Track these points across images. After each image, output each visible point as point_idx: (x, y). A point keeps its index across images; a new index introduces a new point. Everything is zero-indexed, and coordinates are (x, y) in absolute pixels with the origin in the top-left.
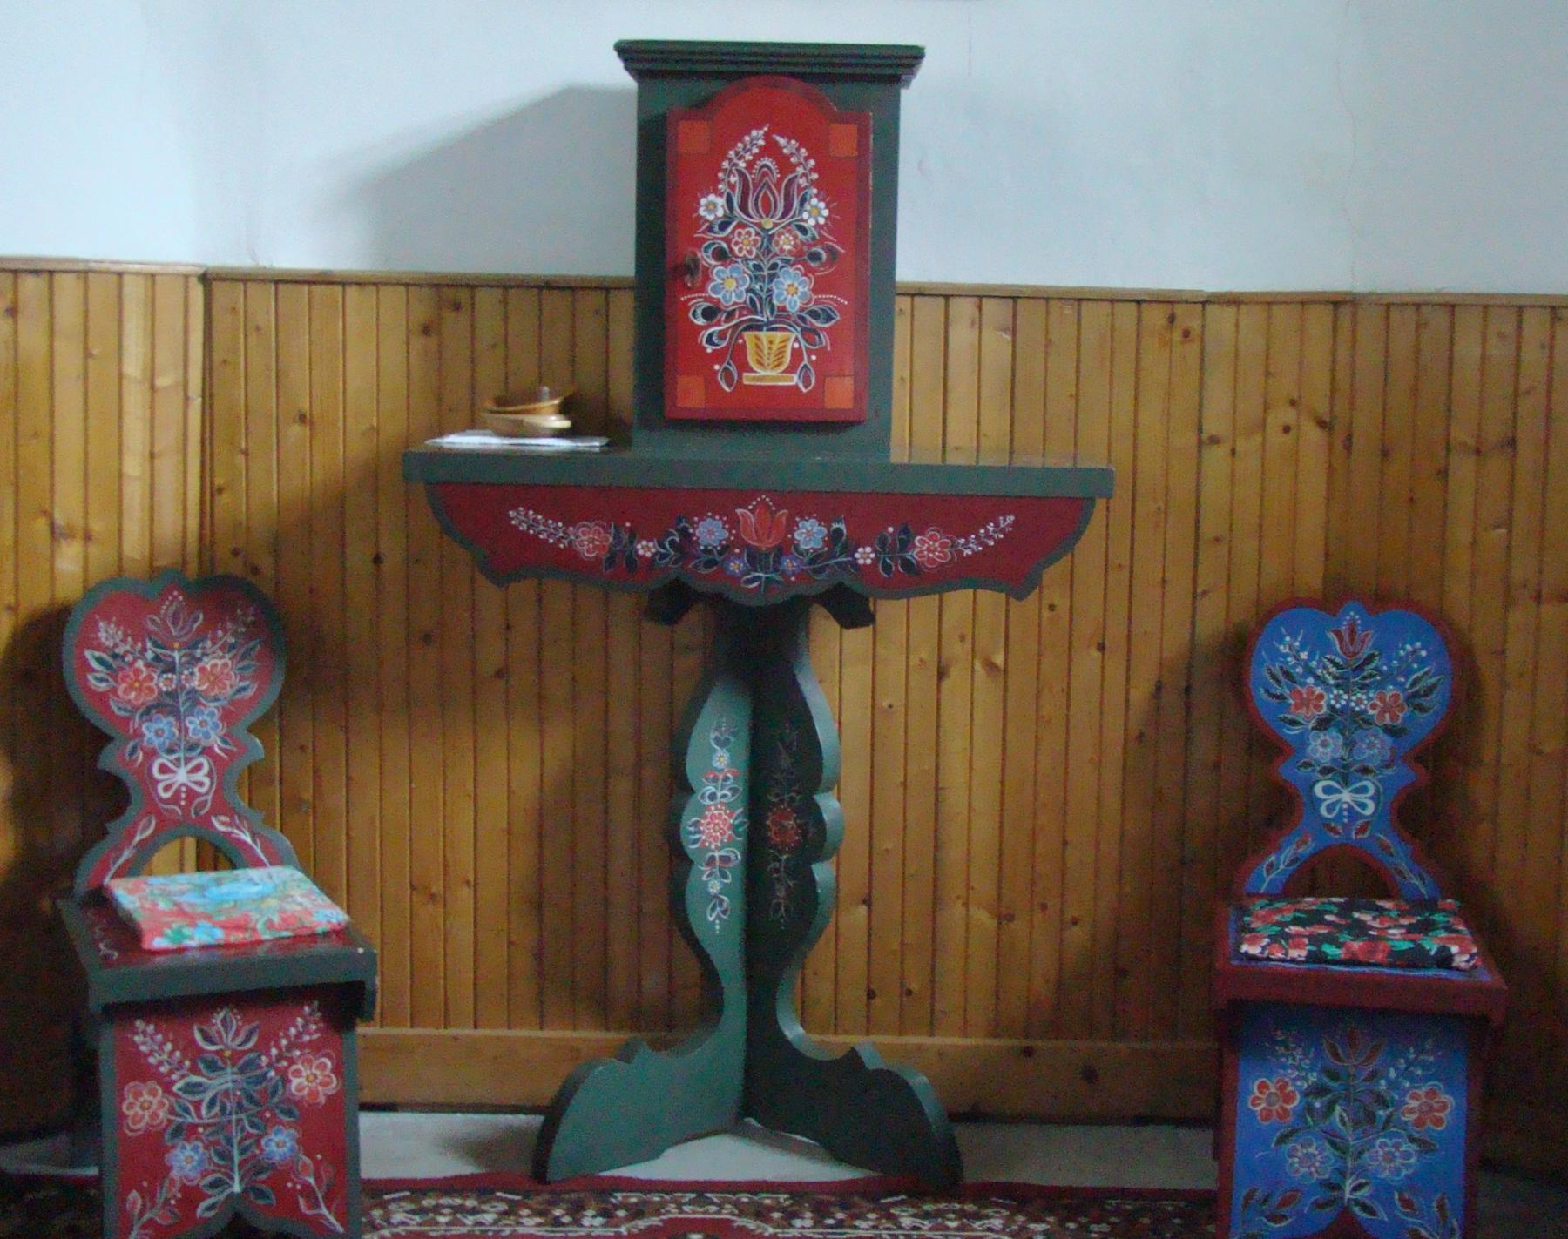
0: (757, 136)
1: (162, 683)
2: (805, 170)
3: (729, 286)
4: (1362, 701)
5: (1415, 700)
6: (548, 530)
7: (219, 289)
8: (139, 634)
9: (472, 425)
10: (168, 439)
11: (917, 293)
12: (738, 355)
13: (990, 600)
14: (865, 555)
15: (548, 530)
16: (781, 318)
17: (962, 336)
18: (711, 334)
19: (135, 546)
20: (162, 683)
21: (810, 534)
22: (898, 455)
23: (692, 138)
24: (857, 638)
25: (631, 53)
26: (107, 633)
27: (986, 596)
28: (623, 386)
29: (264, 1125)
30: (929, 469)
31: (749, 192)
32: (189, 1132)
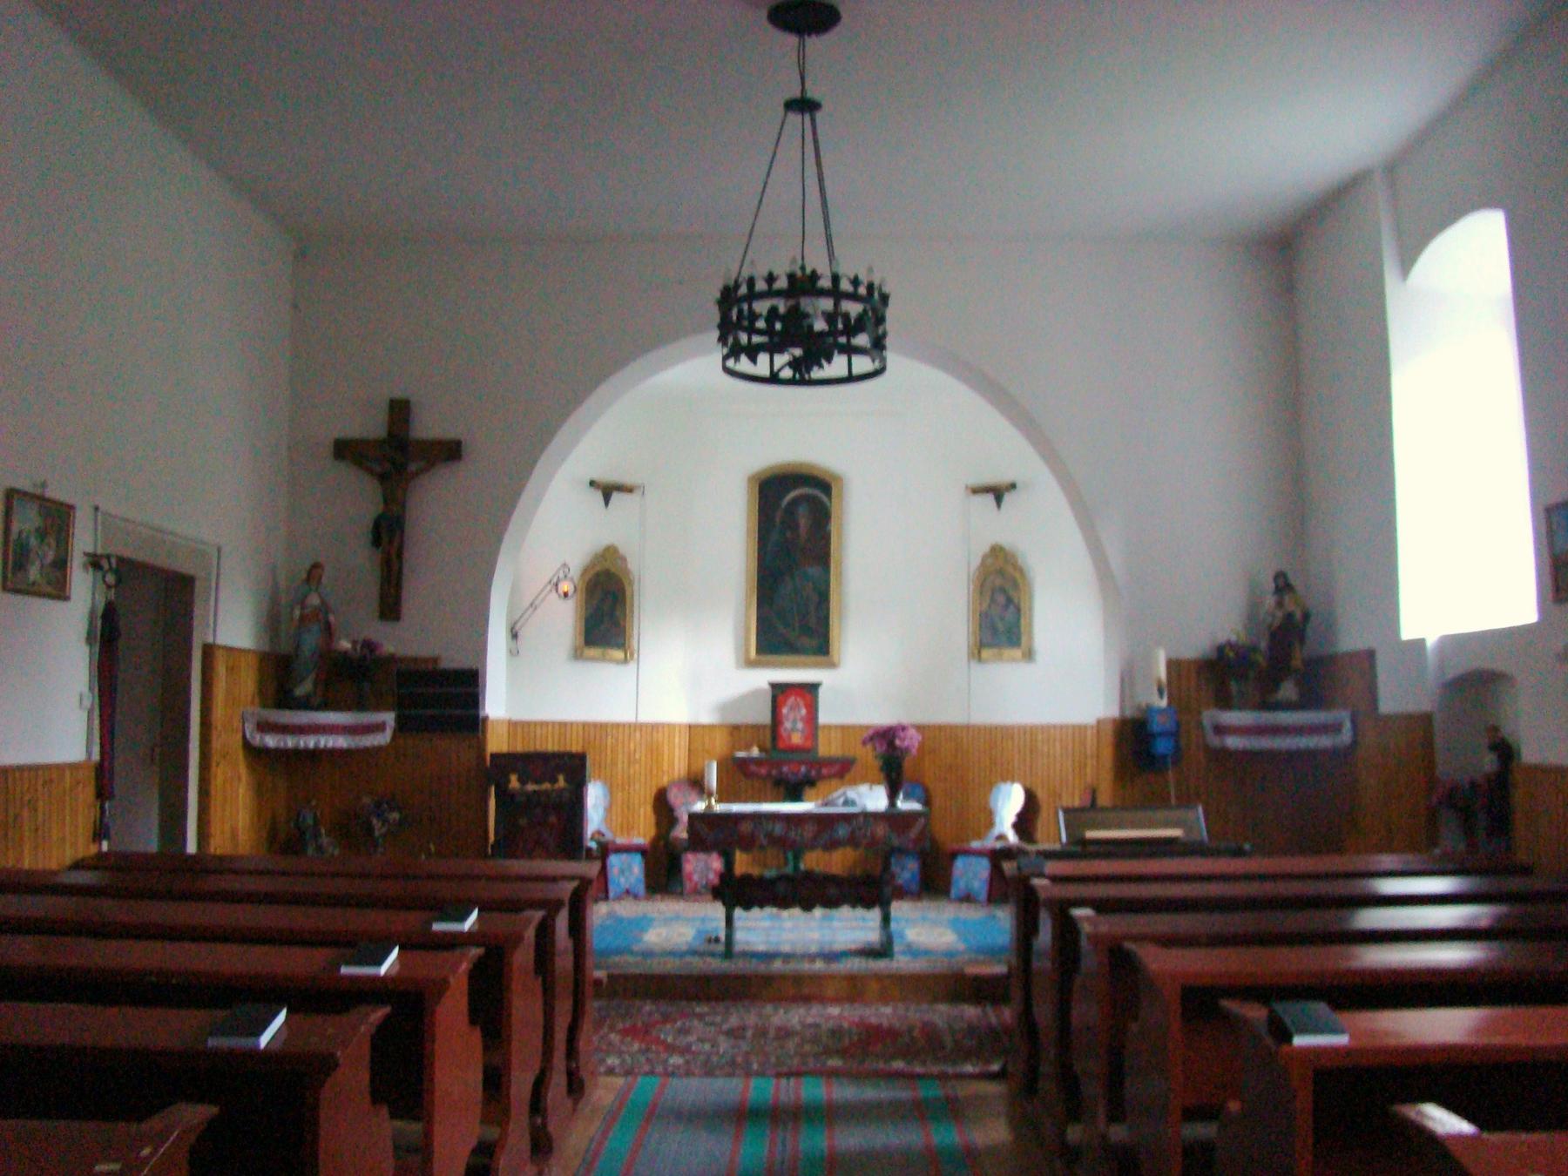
2: (801, 703)
3: (788, 725)
7: (692, 729)
8: (679, 789)
9: (740, 750)
10: (682, 757)
11: (824, 727)
12: (789, 737)
16: (798, 730)
17: (833, 735)
18: (784, 734)
19: (676, 775)
23: (780, 698)
28: (768, 744)
31: (792, 708)
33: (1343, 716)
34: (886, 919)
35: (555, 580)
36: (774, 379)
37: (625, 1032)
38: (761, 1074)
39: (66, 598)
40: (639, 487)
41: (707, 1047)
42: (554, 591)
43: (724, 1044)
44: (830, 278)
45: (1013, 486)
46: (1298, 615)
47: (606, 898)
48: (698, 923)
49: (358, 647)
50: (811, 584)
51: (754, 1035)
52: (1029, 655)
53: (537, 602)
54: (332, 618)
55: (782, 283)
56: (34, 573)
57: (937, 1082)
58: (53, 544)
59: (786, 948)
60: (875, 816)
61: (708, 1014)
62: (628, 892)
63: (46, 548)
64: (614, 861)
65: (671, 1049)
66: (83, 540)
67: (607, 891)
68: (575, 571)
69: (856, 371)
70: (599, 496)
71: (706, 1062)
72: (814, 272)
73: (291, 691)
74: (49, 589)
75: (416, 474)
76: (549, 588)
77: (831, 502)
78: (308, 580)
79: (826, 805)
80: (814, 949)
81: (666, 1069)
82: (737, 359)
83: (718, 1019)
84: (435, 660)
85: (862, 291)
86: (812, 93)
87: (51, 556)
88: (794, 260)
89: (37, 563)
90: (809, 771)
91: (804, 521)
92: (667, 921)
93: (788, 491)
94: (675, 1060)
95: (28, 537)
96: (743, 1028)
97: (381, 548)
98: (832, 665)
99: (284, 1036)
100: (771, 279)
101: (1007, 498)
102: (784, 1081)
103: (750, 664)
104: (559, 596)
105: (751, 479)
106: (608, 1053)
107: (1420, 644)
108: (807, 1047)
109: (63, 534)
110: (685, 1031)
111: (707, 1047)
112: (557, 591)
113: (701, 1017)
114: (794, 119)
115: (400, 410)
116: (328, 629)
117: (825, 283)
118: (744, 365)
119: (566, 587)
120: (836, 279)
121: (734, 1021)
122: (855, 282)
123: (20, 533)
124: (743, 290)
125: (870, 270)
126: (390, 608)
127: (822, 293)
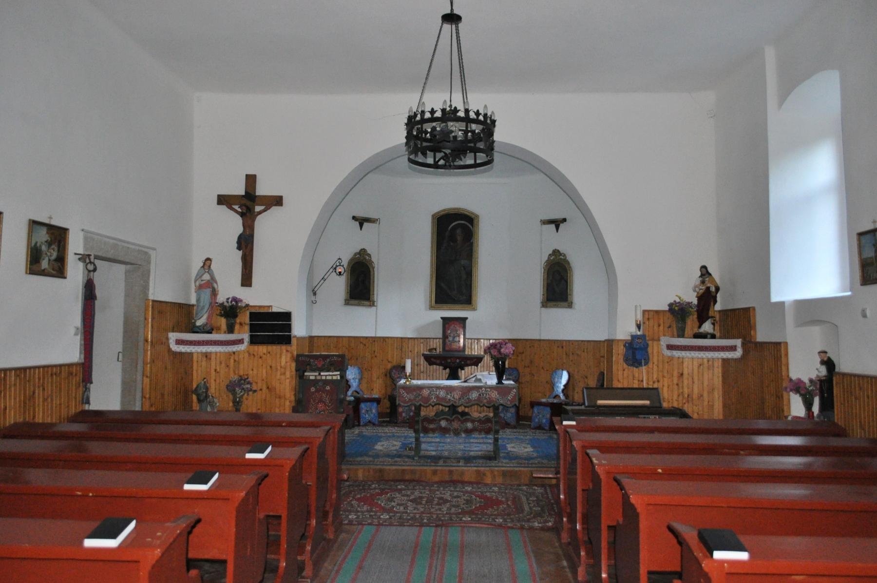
0: (453, 325)
1: (399, 376)
4: (510, 377)
5: (515, 377)
6: (434, 360)
11: (468, 339)
12: (451, 344)
13: (476, 367)
14: (463, 363)
15: (434, 360)
20: (399, 376)
21: (458, 361)
22: (466, 353)
24: (463, 371)
25: (442, 318)
26: (394, 371)
27: (473, 367)
29: (410, 412)
30: (470, 355)
32: (404, 412)
33: (738, 342)
34: (496, 440)
35: (334, 266)
36: (436, 166)
37: (359, 500)
38: (427, 525)
39: (65, 278)
40: (377, 220)
41: (402, 508)
42: (334, 273)
43: (411, 507)
44: (464, 111)
45: (564, 220)
46: (713, 289)
47: (359, 425)
48: (403, 439)
49: (230, 300)
50: (462, 268)
51: (427, 502)
52: (570, 305)
53: (326, 277)
54: (215, 285)
55: (438, 114)
56: (45, 264)
57: (519, 531)
58: (56, 249)
59: (446, 454)
60: (491, 388)
61: (405, 490)
62: (370, 422)
63: (52, 251)
64: (363, 406)
65: (384, 510)
66: (75, 245)
67: (359, 422)
68: (345, 263)
69: (478, 162)
70: (357, 223)
71: (400, 518)
72: (455, 108)
73: (195, 323)
74: (54, 272)
75: (260, 213)
76: (331, 270)
77: (473, 227)
78: (203, 267)
79: (465, 382)
80: (460, 454)
81: (379, 522)
82: (416, 155)
83: (409, 493)
84: (269, 307)
85: (481, 118)
86: (456, 12)
87: (55, 255)
88: (445, 101)
89: (47, 259)
90: (460, 362)
91: (459, 238)
92: (388, 438)
93: (452, 223)
94: (385, 516)
95: (40, 246)
96: (421, 498)
97: (242, 251)
98: (474, 309)
99: (134, 535)
100: (433, 112)
101: (562, 226)
102: (439, 529)
103: (432, 308)
104: (337, 274)
105: (433, 216)
106: (350, 512)
107: (781, 304)
108: (453, 510)
109: (62, 243)
110: (391, 500)
111: (402, 508)
112: (335, 272)
113: (400, 491)
114: (447, 27)
115: (251, 180)
116: (214, 293)
117: (461, 114)
118: (420, 159)
119: (339, 270)
120: (467, 111)
121: (417, 493)
122: (478, 113)
123: (36, 243)
124: (418, 118)
125: (486, 107)
126: (247, 280)
127: (460, 119)
